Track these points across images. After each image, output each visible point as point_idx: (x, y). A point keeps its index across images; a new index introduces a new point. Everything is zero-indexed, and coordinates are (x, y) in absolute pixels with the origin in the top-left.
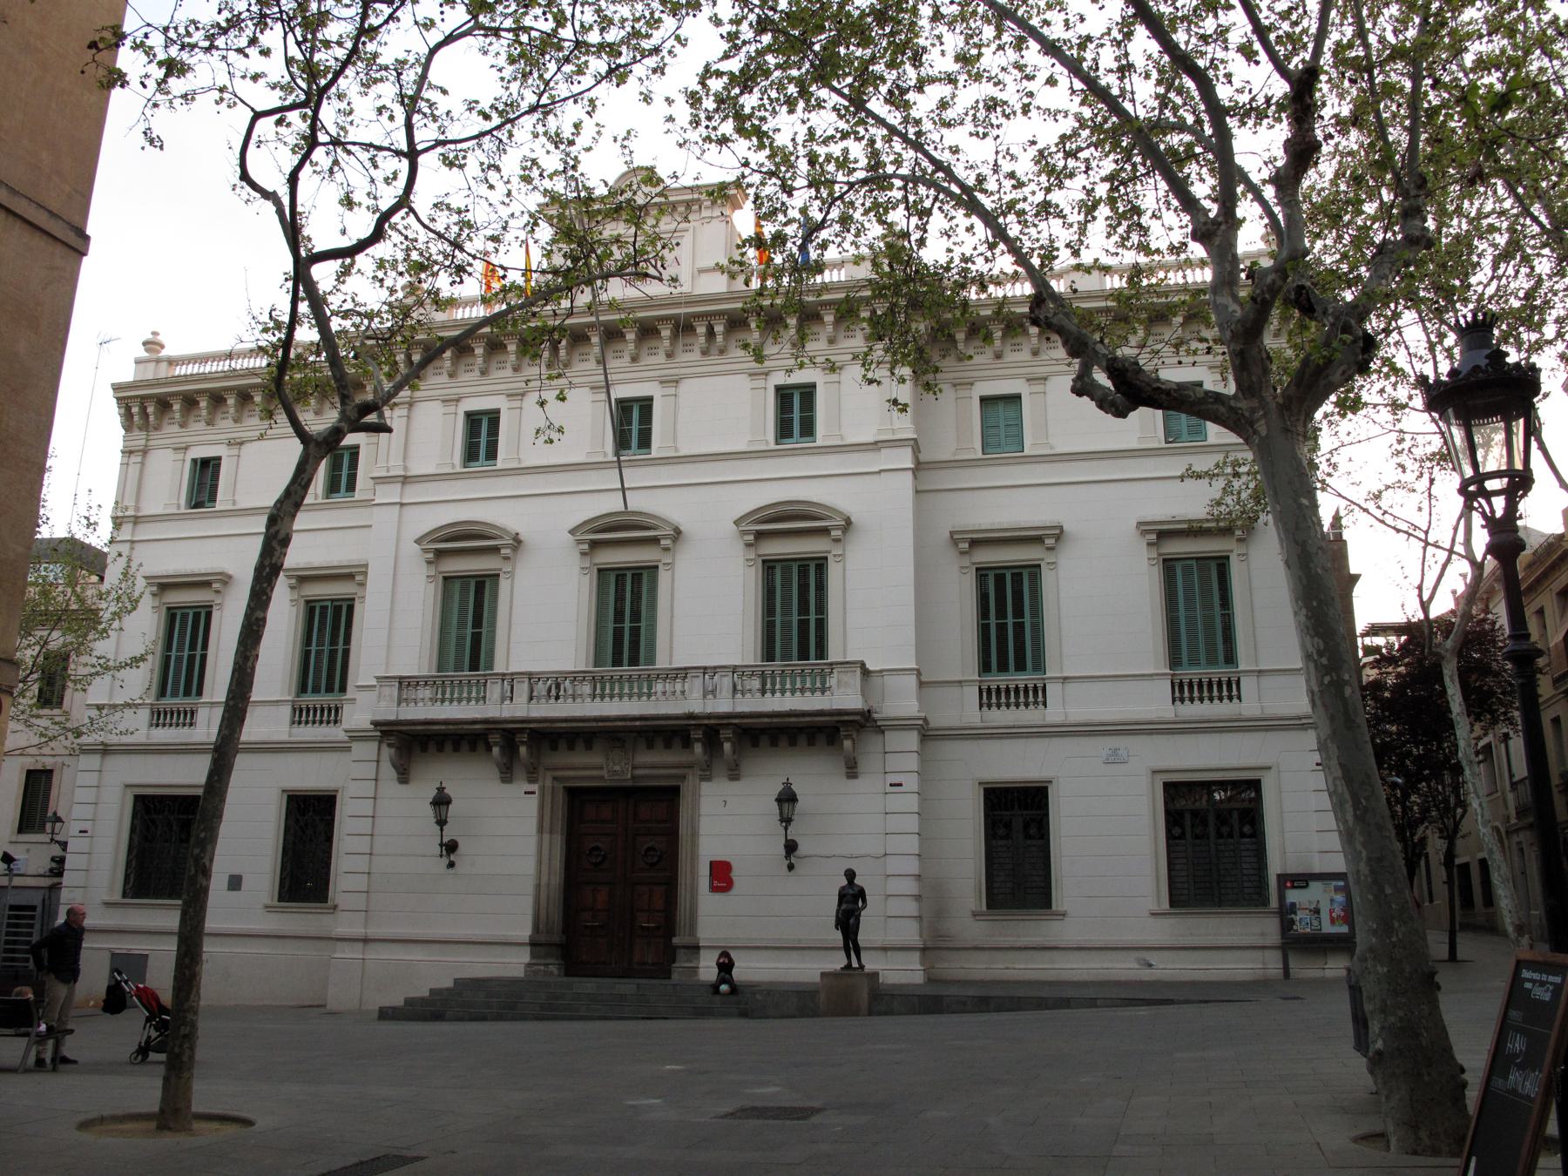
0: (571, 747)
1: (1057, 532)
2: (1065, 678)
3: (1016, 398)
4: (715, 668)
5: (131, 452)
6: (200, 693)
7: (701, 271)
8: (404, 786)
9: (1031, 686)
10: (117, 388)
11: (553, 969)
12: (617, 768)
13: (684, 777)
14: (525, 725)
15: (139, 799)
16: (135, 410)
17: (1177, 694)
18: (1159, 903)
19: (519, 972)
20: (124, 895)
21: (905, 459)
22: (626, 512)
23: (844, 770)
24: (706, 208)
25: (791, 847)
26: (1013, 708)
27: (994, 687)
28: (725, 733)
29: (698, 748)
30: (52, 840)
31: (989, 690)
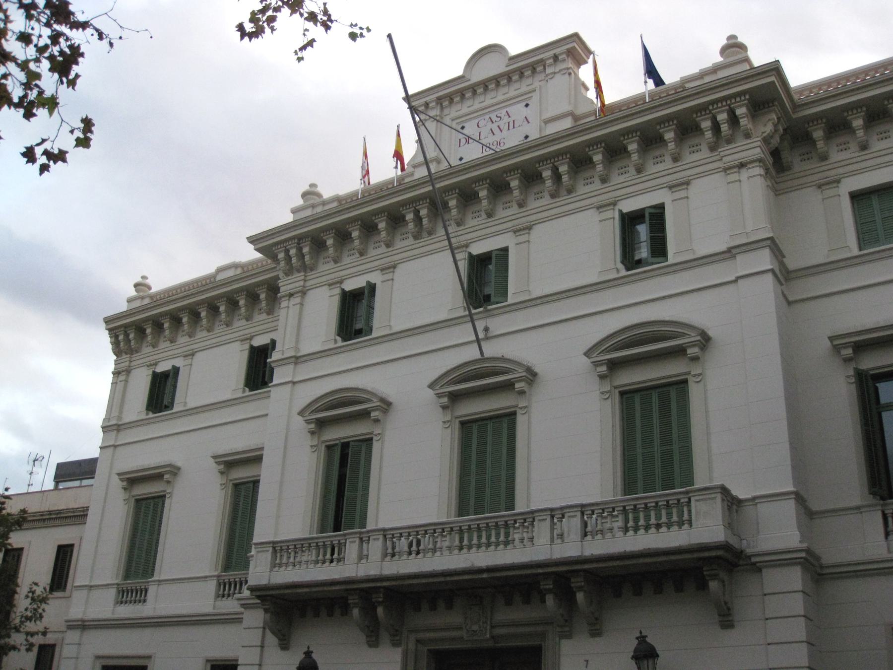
0: (433, 608)
4: (562, 508)
6: (152, 575)
7: (547, 122)
10: (108, 321)
12: (475, 627)
13: (543, 635)
14: (379, 584)
21: (764, 260)
22: (483, 359)
24: (550, 65)
29: (550, 600)
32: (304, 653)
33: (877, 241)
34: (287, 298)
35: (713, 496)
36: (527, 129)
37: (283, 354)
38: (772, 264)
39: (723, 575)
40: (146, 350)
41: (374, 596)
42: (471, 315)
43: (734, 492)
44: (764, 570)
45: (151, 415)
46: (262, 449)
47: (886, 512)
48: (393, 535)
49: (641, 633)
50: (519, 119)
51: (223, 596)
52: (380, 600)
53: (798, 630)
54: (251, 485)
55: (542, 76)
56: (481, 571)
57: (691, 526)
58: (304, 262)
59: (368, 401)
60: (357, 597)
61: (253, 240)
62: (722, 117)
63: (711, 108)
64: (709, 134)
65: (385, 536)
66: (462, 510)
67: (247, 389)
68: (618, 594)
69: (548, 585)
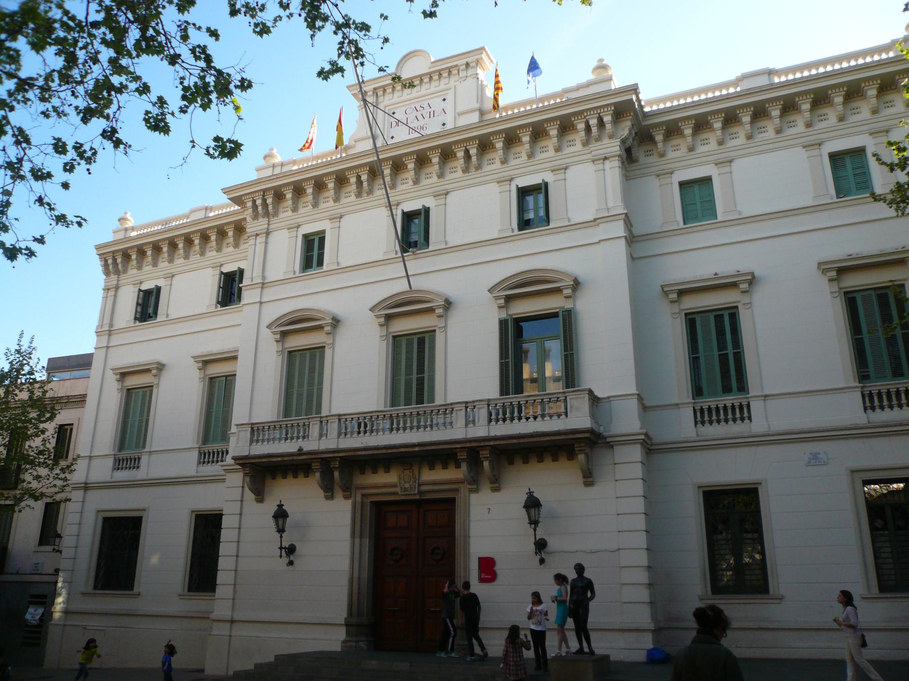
0: (375, 471)
1: (749, 277)
2: (766, 396)
3: (707, 180)
4: (474, 402)
5: (108, 289)
6: (144, 447)
7: (460, 114)
8: (260, 505)
9: (737, 404)
10: (98, 247)
11: (363, 645)
12: (407, 485)
13: (457, 490)
14: (336, 455)
15: (106, 520)
16: (110, 261)
17: (868, 404)
18: (869, 587)
19: (337, 647)
20: (95, 588)
21: (618, 229)
23: (581, 479)
25: (541, 545)
26: (723, 423)
27: (705, 407)
28: (485, 453)
29: (464, 466)
30: (54, 549)
31: (702, 410)
32: (277, 506)
33: (696, 218)
34: (254, 237)
35: (582, 396)
36: (442, 118)
37: (252, 281)
38: (625, 233)
39: (588, 450)
40: (132, 272)
41: (332, 463)
42: (403, 257)
43: (596, 393)
44: (615, 447)
45: (138, 323)
46: (237, 351)
47: (696, 408)
48: (346, 419)
49: (529, 489)
50: (438, 110)
51: (204, 463)
52: (337, 466)
53: (638, 488)
54: (224, 378)
55: (457, 77)
56: (414, 445)
57: (567, 417)
58: (268, 210)
59: (323, 319)
60: (319, 464)
61: (226, 191)
62: (593, 122)
63: (585, 114)
64: (583, 134)
65: (340, 420)
66: (394, 402)
67: (219, 306)
68: (511, 462)
69: (463, 456)
